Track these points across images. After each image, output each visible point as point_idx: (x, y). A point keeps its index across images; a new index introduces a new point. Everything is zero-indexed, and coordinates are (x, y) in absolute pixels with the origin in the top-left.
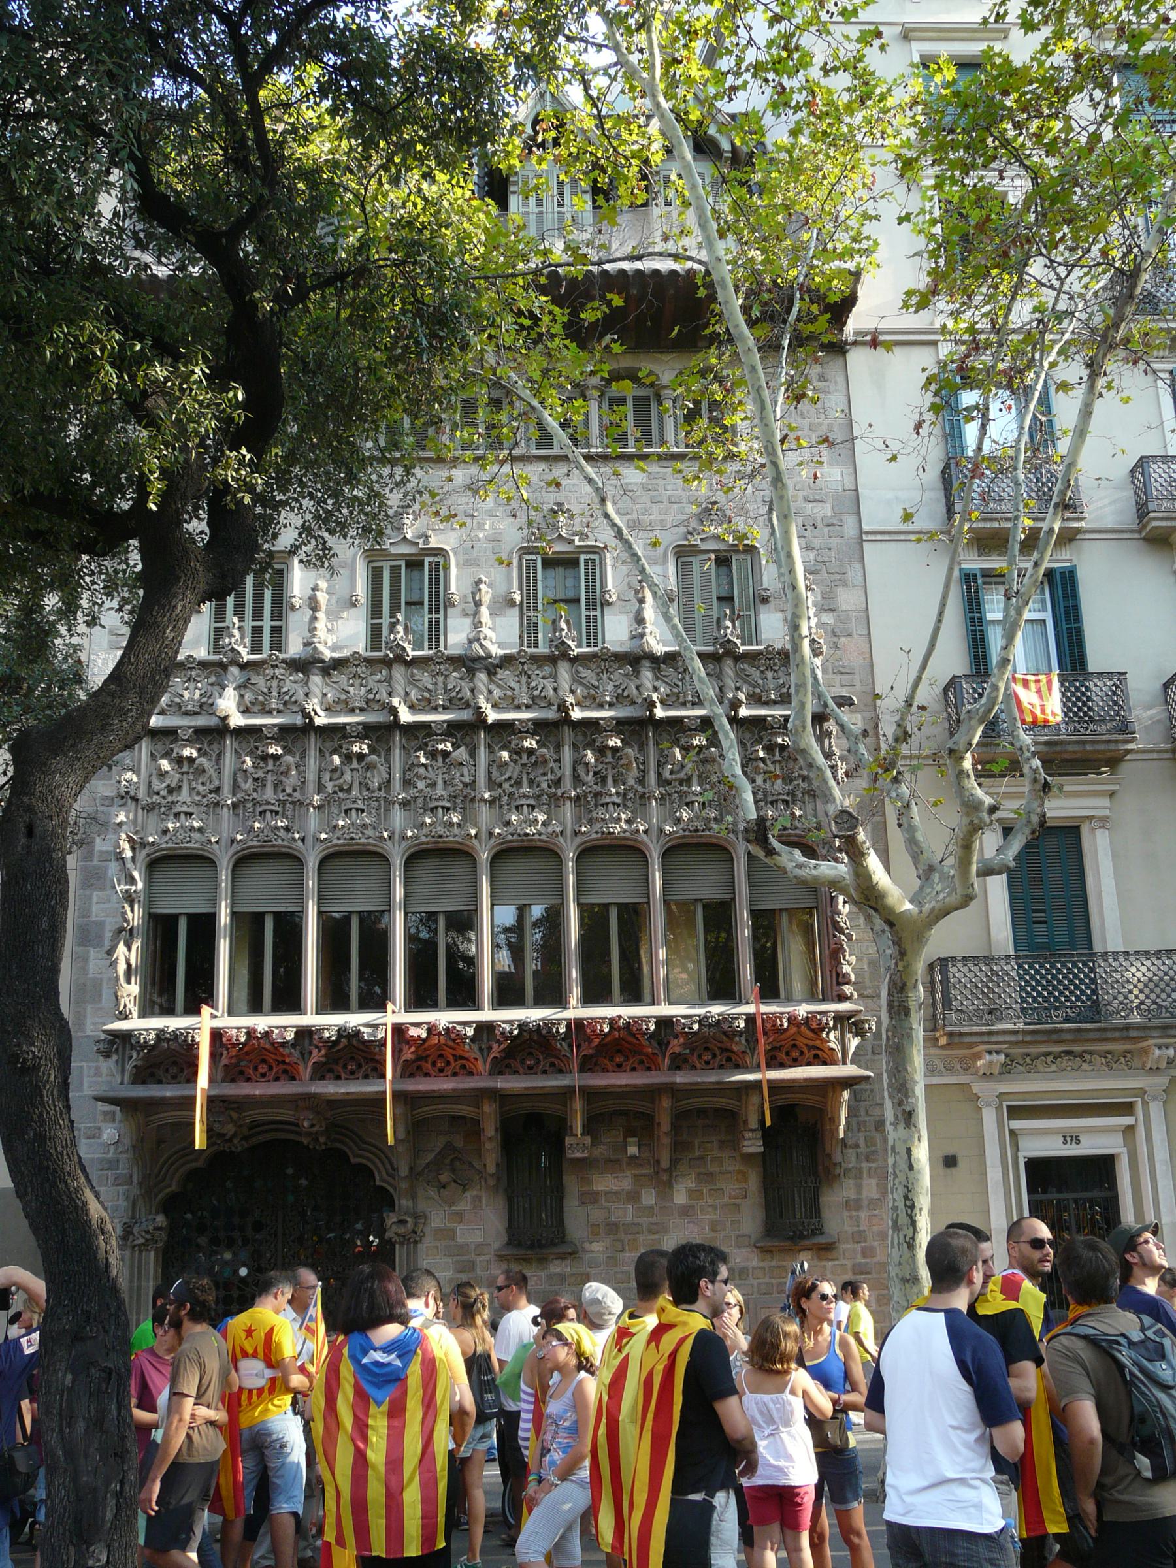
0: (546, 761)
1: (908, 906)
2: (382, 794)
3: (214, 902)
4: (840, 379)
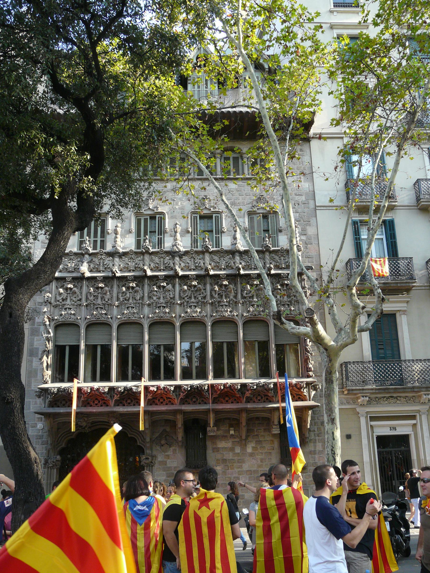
0: (200, 290)
1: (332, 343)
2: (141, 301)
3: (79, 341)
4: (308, 151)
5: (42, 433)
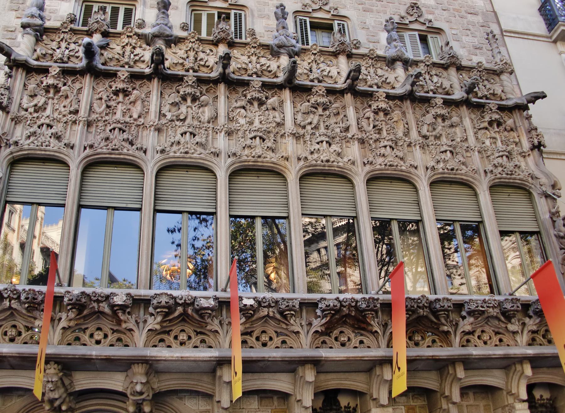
2: (211, 125)
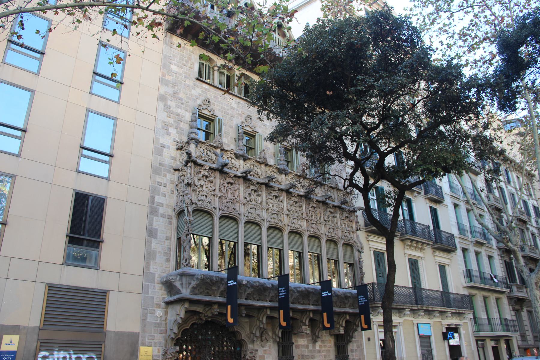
5: (160, 320)
